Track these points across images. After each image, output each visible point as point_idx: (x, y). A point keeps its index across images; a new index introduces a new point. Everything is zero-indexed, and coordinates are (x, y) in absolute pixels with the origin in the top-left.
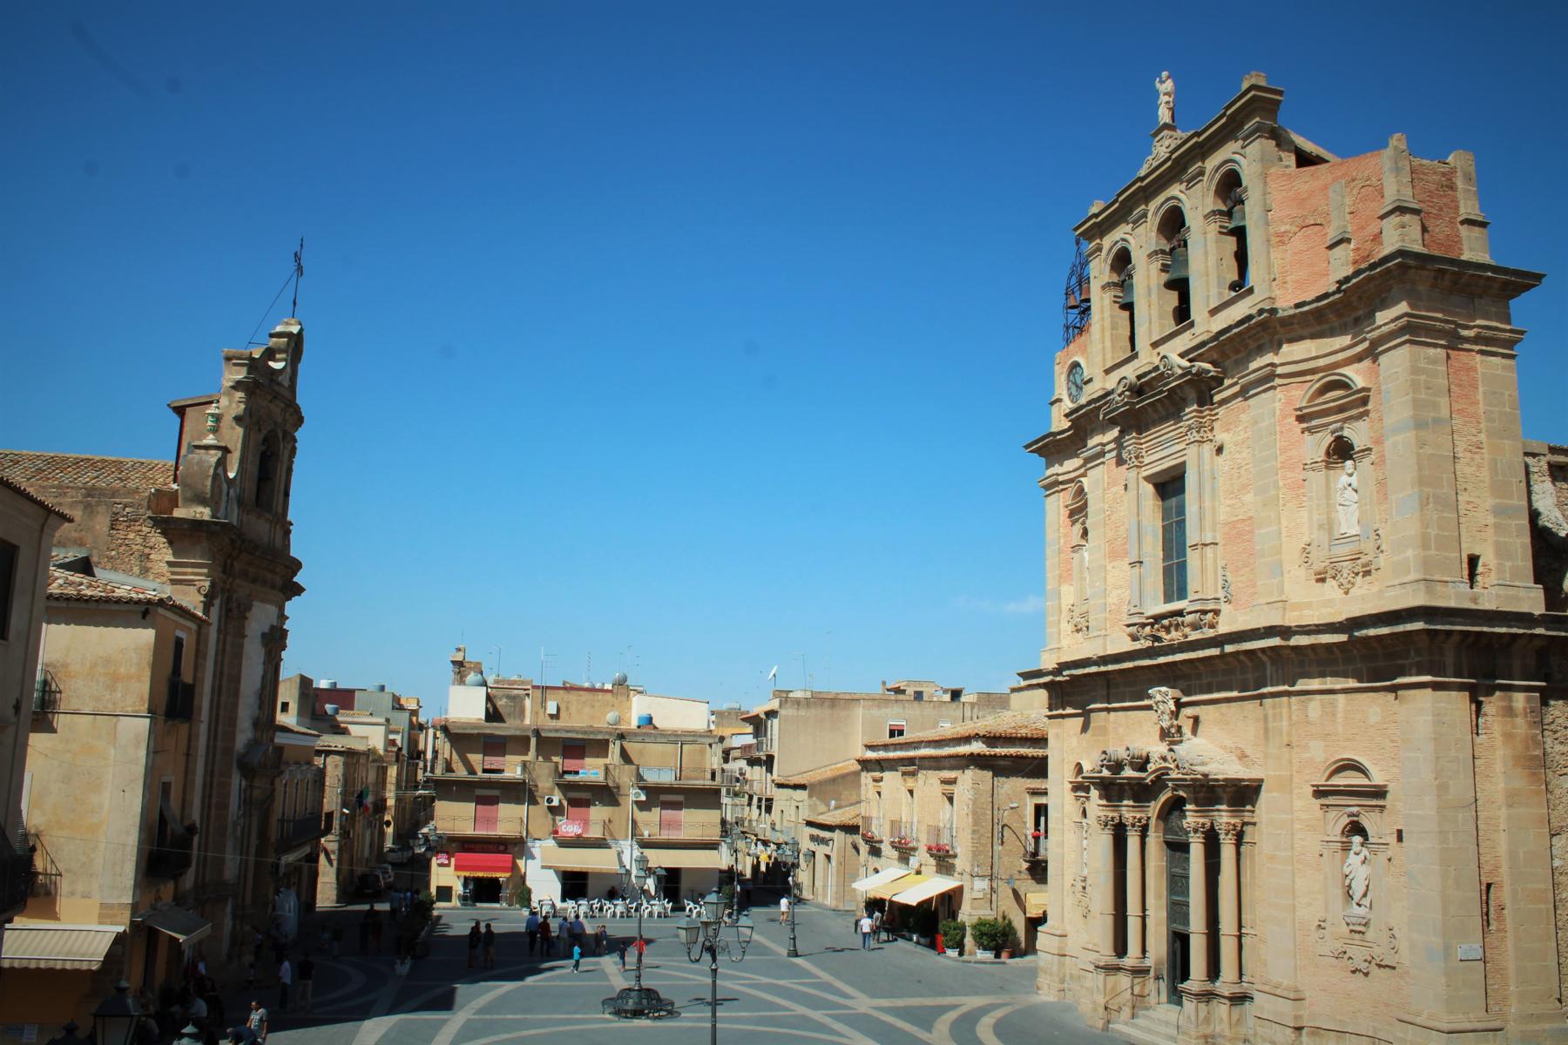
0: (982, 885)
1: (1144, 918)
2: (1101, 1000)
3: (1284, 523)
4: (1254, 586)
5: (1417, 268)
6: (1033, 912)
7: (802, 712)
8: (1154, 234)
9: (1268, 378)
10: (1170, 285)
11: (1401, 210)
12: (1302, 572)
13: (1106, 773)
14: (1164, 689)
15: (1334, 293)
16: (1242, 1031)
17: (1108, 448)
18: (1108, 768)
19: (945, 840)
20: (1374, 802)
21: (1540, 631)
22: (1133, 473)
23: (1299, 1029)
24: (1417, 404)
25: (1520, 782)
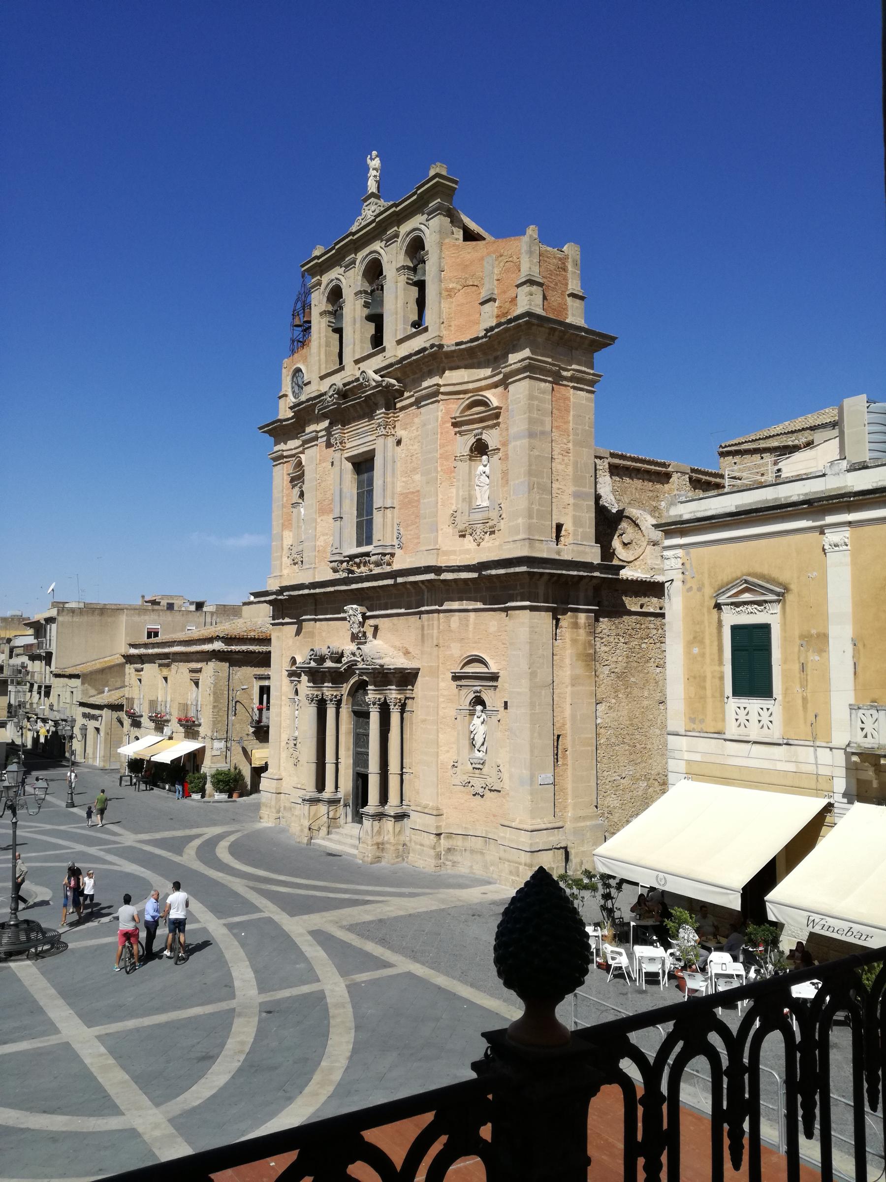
0: (219, 745)
1: (337, 764)
2: (306, 824)
3: (440, 496)
4: (418, 538)
5: (538, 325)
6: (257, 763)
7: (76, 619)
8: (360, 278)
9: (434, 394)
10: (369, 318)
11: (531, 282)
12: (450, 530)
13: (313, 664)
14: (355, 606)
15: (482, 338)
16: (402, 838)
17: (320, 434)
18: (315, 660)
19: (192, 714)
20: (491, 684)
21: (597, 574)
22: (338, 455)
23: (439, 835)
24: (531, 421)
25: (580, 671)
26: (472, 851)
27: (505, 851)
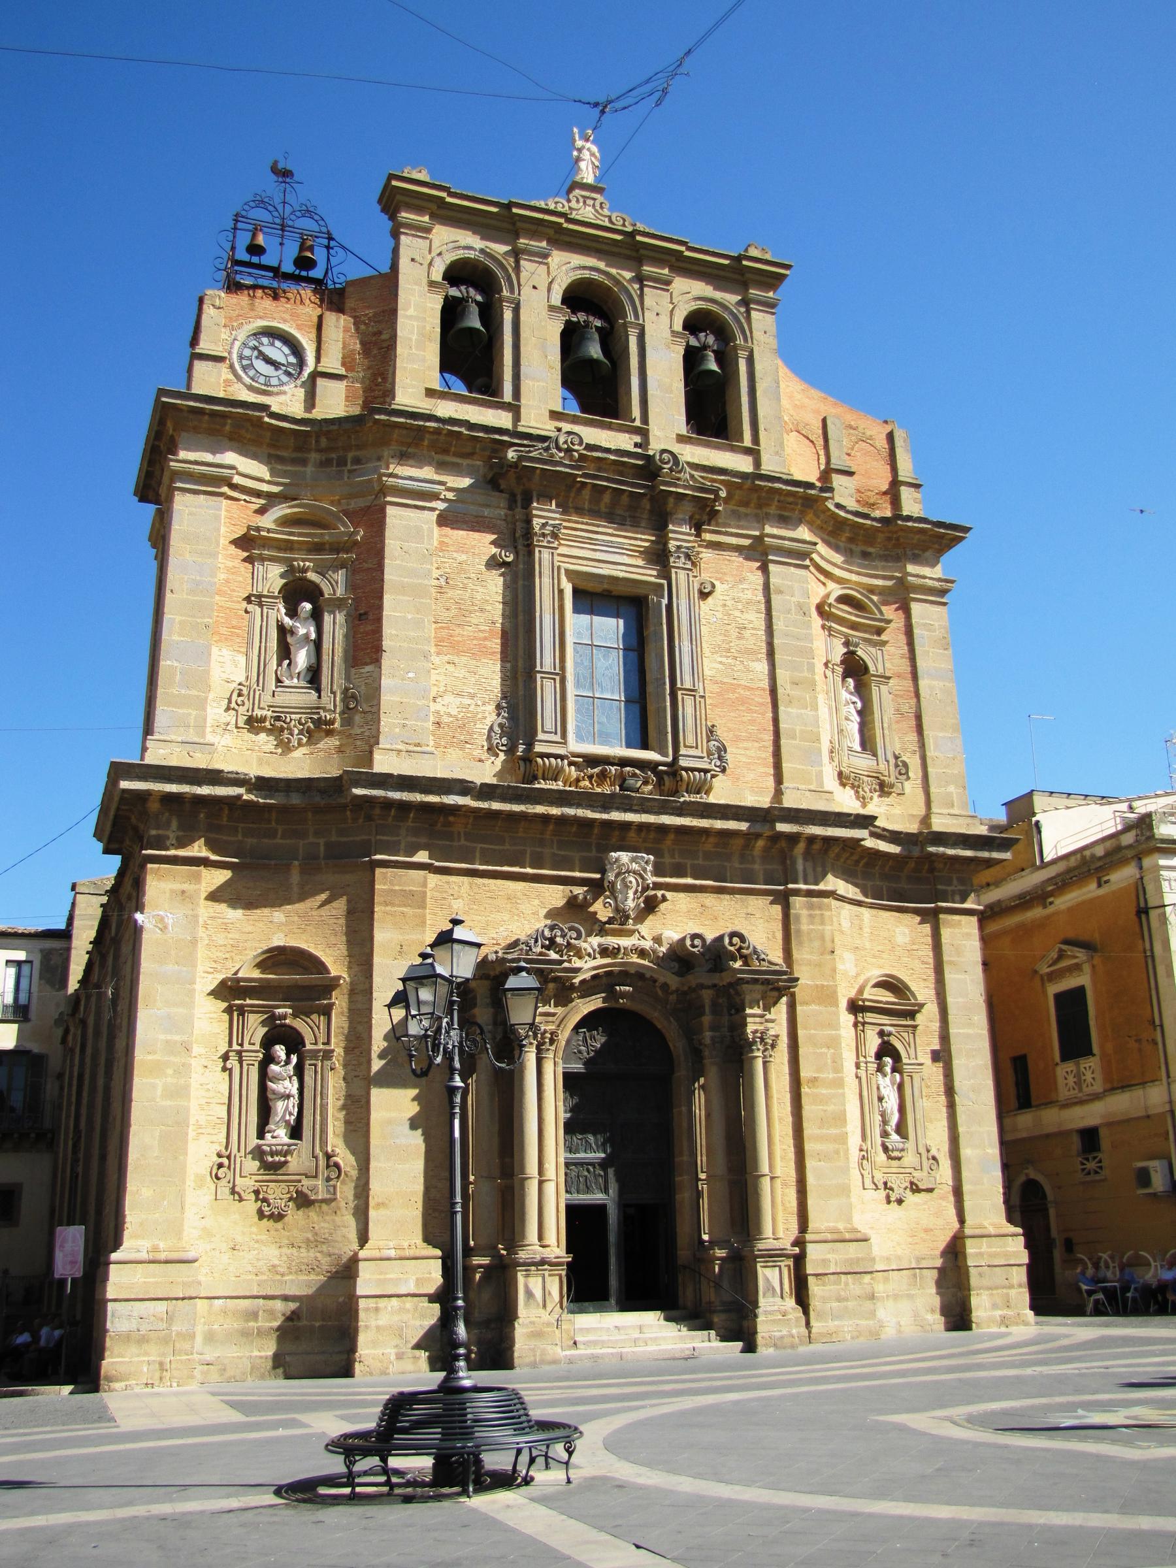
9: (800, 555)
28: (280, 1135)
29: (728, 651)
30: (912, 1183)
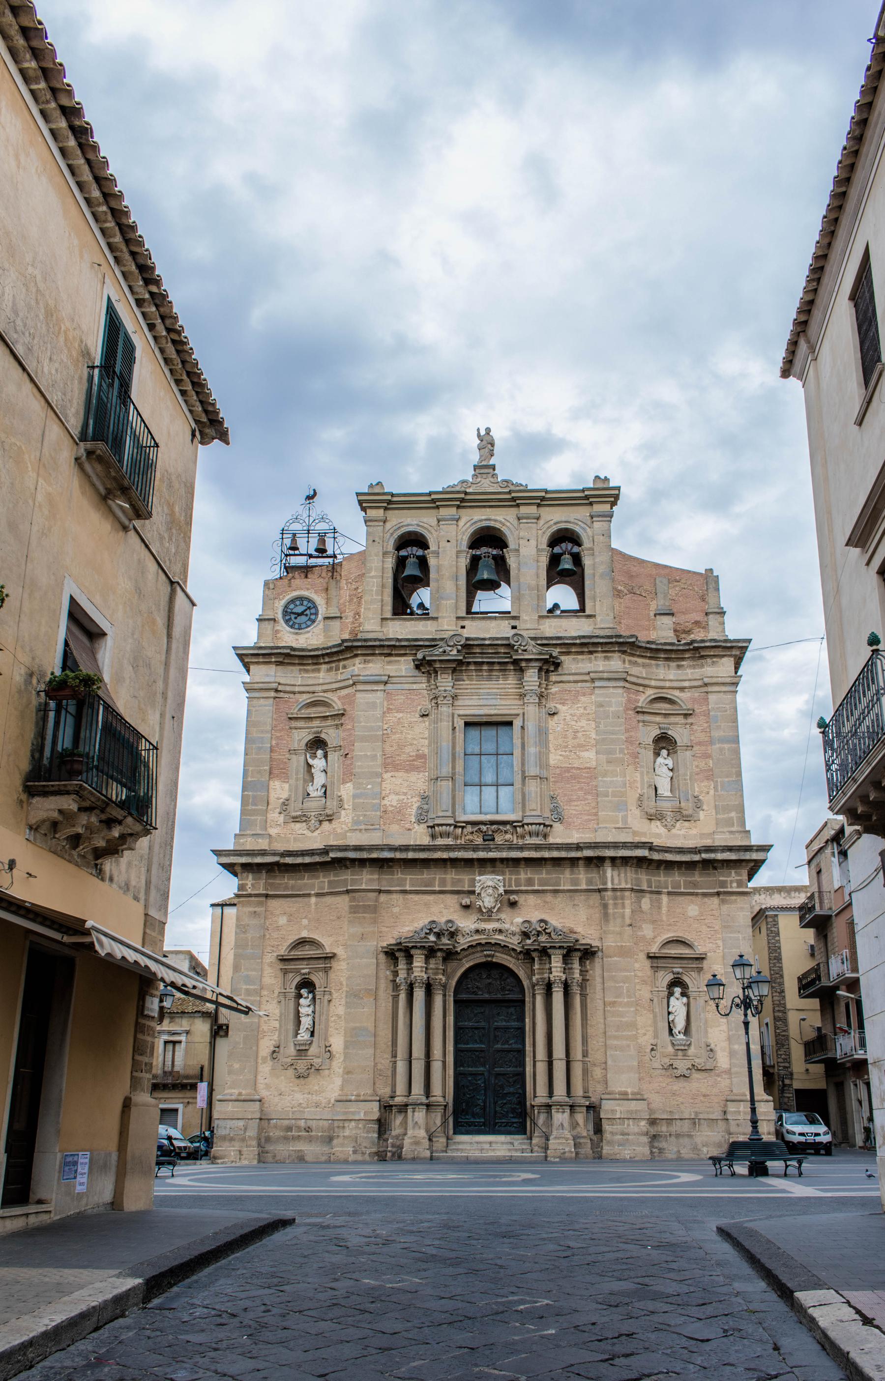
12: (637, 812)
13: (432, 938)
26: (678, 1136)
27: (738, 1125)
28: (304, 1036)
29: (566, 747)
30: (693, 1065)
